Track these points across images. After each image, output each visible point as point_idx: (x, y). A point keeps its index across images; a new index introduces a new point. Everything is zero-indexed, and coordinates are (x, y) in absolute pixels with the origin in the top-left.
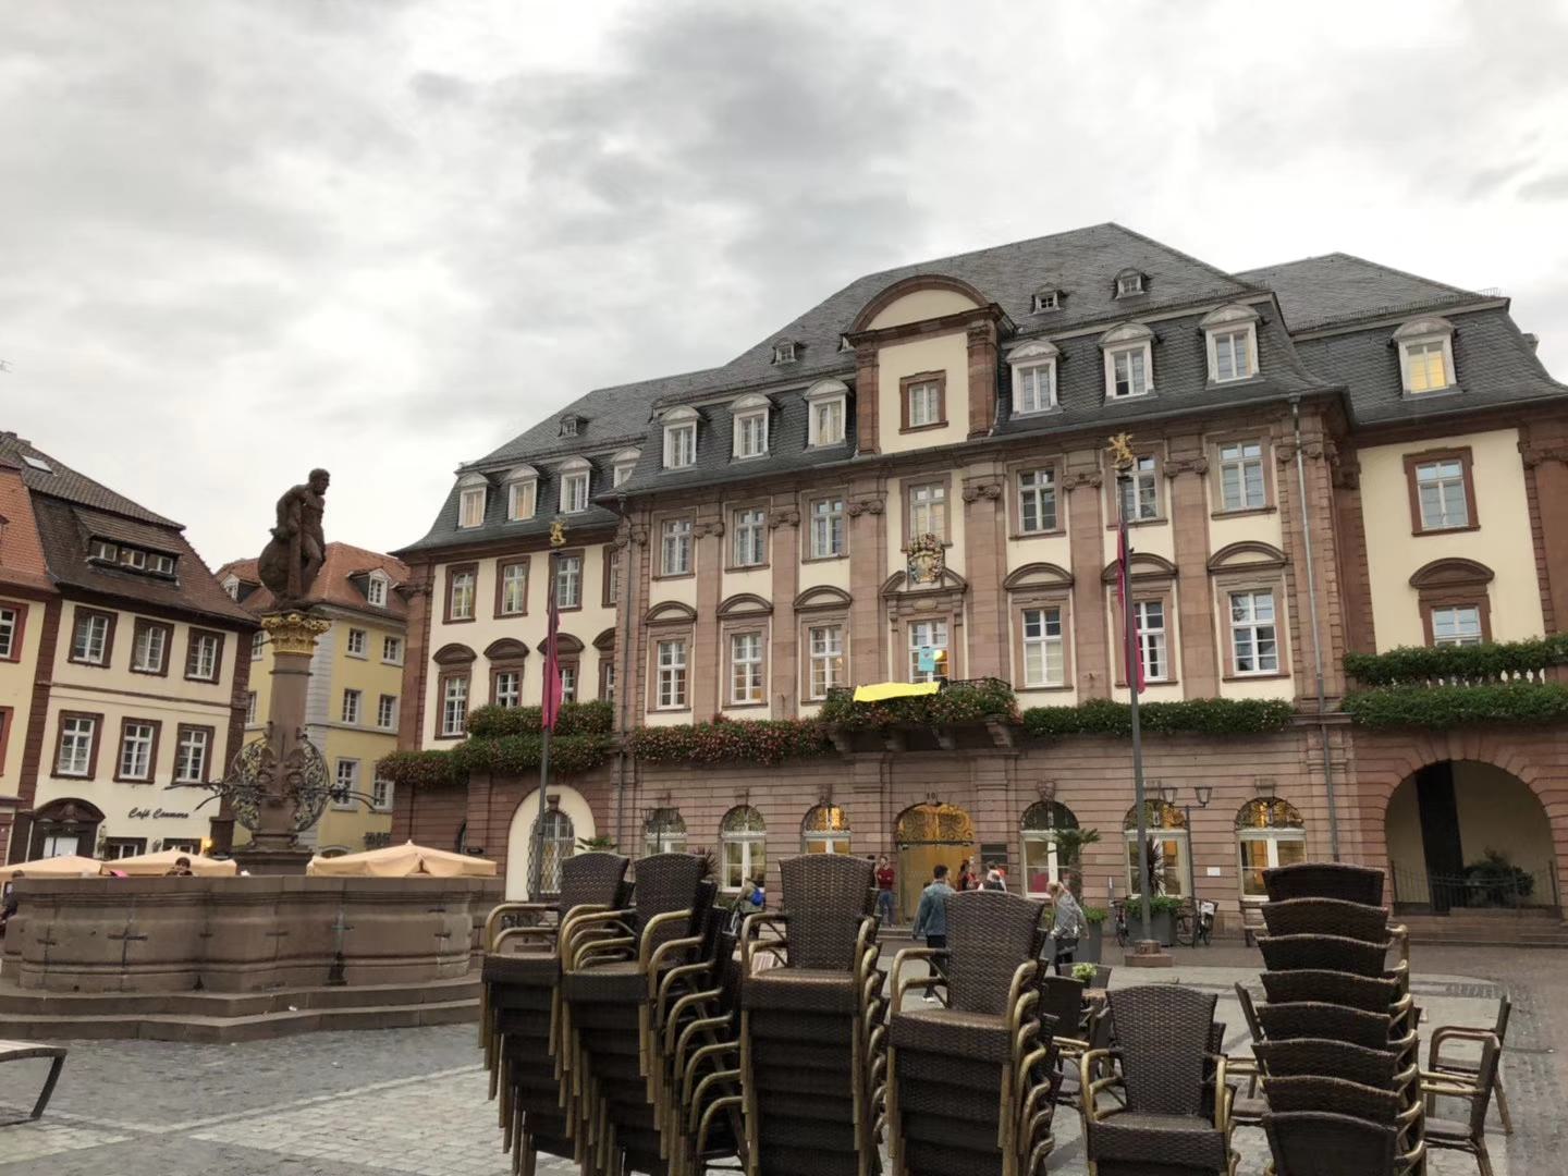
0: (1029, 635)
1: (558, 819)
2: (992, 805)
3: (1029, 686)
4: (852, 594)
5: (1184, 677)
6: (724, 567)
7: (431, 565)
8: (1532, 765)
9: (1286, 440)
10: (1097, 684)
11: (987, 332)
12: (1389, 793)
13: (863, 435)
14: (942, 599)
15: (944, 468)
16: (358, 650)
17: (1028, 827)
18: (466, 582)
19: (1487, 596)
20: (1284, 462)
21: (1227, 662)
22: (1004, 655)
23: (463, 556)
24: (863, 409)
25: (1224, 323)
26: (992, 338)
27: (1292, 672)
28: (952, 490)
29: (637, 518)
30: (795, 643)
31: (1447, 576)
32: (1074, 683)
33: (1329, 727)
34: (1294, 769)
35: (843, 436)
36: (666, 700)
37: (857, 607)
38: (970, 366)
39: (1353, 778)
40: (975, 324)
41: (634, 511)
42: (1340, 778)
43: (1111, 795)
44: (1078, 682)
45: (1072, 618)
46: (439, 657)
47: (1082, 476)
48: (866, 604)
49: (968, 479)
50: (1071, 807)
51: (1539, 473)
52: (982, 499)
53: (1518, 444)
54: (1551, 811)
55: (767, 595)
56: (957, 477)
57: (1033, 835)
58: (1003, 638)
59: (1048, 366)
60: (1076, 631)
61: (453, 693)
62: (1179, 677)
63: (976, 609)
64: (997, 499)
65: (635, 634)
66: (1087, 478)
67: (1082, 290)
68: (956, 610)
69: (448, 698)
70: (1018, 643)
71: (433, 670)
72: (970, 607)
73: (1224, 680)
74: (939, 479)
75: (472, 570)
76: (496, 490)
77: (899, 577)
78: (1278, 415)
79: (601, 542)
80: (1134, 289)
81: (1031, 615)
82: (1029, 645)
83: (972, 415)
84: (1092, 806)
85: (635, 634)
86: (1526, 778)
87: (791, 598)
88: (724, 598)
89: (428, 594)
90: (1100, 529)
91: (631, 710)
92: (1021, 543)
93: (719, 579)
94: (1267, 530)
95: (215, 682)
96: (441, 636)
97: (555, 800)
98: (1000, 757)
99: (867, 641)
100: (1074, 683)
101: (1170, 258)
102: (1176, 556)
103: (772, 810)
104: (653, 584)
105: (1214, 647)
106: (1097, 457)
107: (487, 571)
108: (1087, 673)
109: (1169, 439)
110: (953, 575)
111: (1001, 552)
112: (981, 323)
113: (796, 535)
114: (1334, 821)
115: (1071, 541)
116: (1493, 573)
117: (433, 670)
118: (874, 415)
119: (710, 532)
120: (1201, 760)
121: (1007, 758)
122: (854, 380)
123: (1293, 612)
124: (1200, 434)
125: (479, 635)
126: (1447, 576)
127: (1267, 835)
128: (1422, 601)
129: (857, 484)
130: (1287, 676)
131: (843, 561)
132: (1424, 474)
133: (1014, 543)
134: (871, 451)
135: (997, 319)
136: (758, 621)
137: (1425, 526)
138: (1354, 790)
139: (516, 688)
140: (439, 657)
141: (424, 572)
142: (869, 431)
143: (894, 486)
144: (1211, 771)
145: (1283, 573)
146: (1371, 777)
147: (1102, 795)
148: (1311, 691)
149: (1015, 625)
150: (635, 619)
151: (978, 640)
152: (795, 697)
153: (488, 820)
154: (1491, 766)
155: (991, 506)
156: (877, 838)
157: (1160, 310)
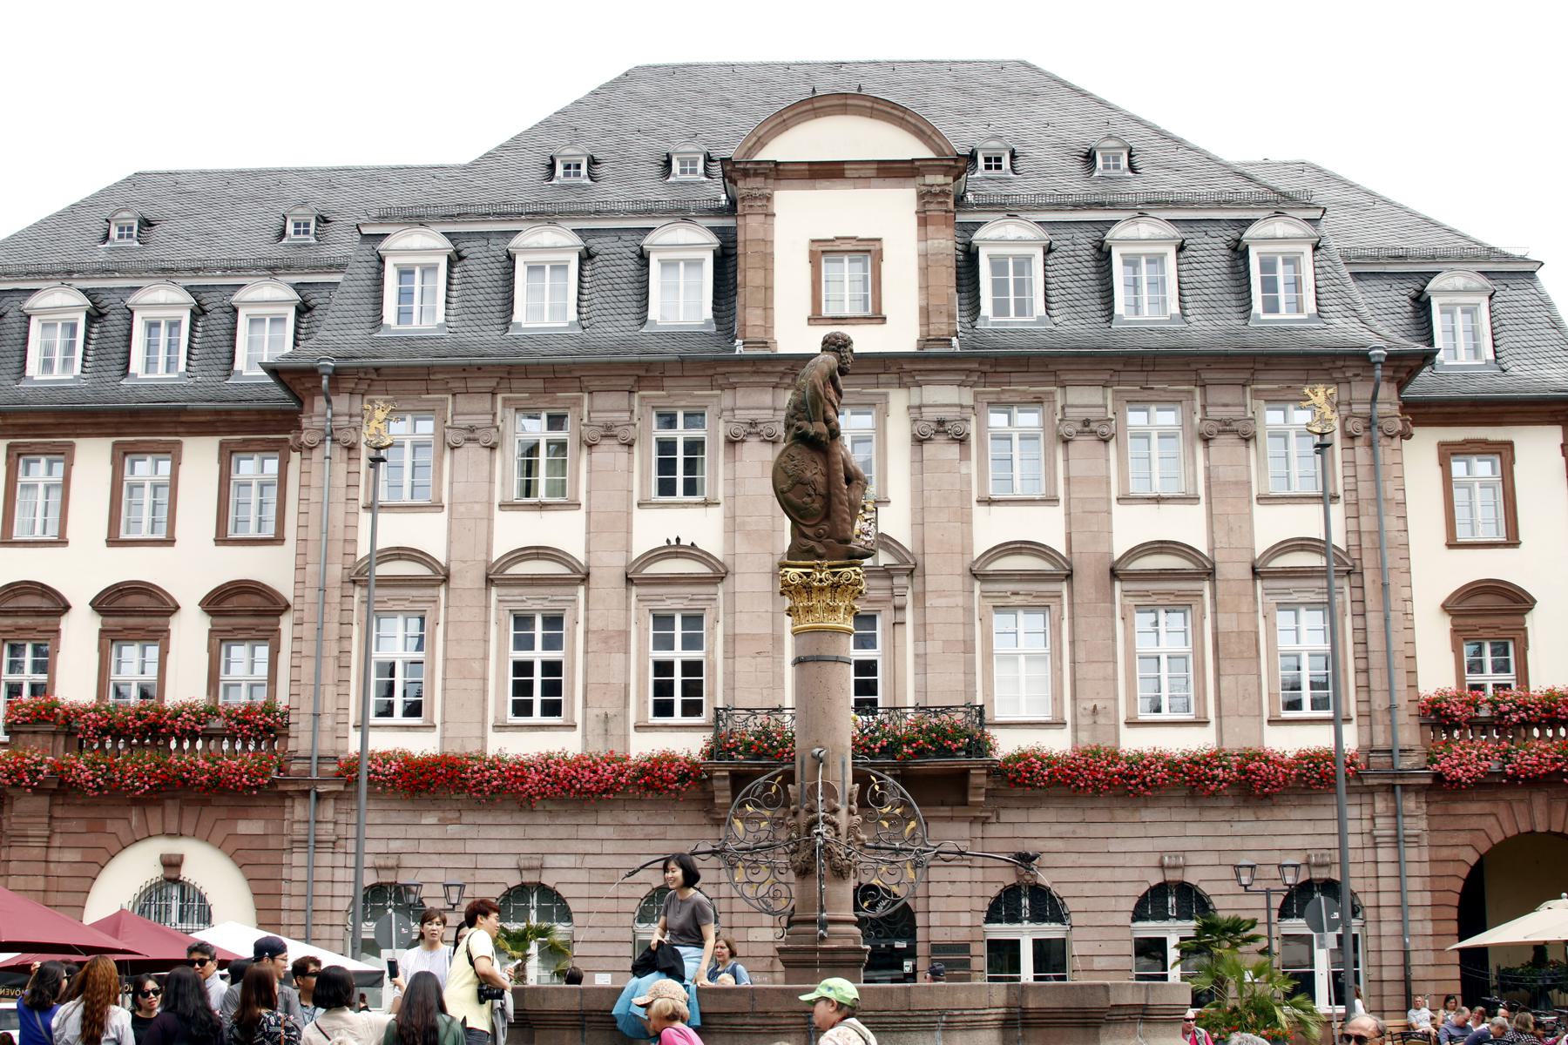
2: (949, 889)
4: (728, 562)
5: (1219, 716)
6: (497, 500)
10: (1101, 720)
12: (1464, 871)
13: (750, 317)
15: (878, 385)
17: (989, 920)
19: (1525, 630)
20: (1352, 438)
22: (969, 672)
24: (748, 275)
25: (1273, 239)
27: (1353, 714)
28: (889, 420)
29: (341, 403)
30: (626, 634)
32: (1068, 718)
33: (1405, 788)
35: (708, 313)
36: (388, 711)
38: (923, 238)
40: (930, 179)
42: (1411, 853)
43: (1118, 874)
44: (1075, 716)
47: (1086, 423)
49: (920, 407)
50: (1056, 890)
52: (941, 438)
53: (1562, 446)
55: (578, 551)
56: (898, 400)
57: (1002, 931)
59: (1029, 258)
60: (1072, 643)
62: (1211, 715)
64: (962, 440)
66: (1094, 426)
67: (1035, 153)
68: (898, 601)
72: (920, 598)
73: (1270, 722)
74: (867, 400)
78: (1349, 374)
80: (1117, 167)
83: (926, 313)
84: (1087, 889)
85: (334, 596)
88: (636, 554)
90: (1109, 500)
91: (327, 722)
92: (994, 509)
93: (490, 519)
97: (172, 864)
98: (963, 819)
100: (1068, 718)
102: (1212, 549)
103: (584, 890)
105: (1259, 676)
106: (1105, 398)
108: (1090, 706)
109: (1203, 386)
111: (966, 520)
112: (940, 179)
113: (630, 461)
114: (1402, 907)
115: (1068, 514)
116: (1534, 601)
118: (768, 288)
119: (475, 440)
120: (1239, 828)
121: (973, 820)
123: (1360, 637)
129: (740, 392)
131: (711, 510)
132: (1458, 468)
133: (986, 508)
136: (560, 592)
137: (1463, 535)
138: (1426, 869)
139: (39, 667)
142: (759, 312)
144: (1252, 843)
146: (1445, 853)
147: (1104, 874)
148: (1380, 741)
150: (336, 572)
152: (626, 717)
156: (768, 935)
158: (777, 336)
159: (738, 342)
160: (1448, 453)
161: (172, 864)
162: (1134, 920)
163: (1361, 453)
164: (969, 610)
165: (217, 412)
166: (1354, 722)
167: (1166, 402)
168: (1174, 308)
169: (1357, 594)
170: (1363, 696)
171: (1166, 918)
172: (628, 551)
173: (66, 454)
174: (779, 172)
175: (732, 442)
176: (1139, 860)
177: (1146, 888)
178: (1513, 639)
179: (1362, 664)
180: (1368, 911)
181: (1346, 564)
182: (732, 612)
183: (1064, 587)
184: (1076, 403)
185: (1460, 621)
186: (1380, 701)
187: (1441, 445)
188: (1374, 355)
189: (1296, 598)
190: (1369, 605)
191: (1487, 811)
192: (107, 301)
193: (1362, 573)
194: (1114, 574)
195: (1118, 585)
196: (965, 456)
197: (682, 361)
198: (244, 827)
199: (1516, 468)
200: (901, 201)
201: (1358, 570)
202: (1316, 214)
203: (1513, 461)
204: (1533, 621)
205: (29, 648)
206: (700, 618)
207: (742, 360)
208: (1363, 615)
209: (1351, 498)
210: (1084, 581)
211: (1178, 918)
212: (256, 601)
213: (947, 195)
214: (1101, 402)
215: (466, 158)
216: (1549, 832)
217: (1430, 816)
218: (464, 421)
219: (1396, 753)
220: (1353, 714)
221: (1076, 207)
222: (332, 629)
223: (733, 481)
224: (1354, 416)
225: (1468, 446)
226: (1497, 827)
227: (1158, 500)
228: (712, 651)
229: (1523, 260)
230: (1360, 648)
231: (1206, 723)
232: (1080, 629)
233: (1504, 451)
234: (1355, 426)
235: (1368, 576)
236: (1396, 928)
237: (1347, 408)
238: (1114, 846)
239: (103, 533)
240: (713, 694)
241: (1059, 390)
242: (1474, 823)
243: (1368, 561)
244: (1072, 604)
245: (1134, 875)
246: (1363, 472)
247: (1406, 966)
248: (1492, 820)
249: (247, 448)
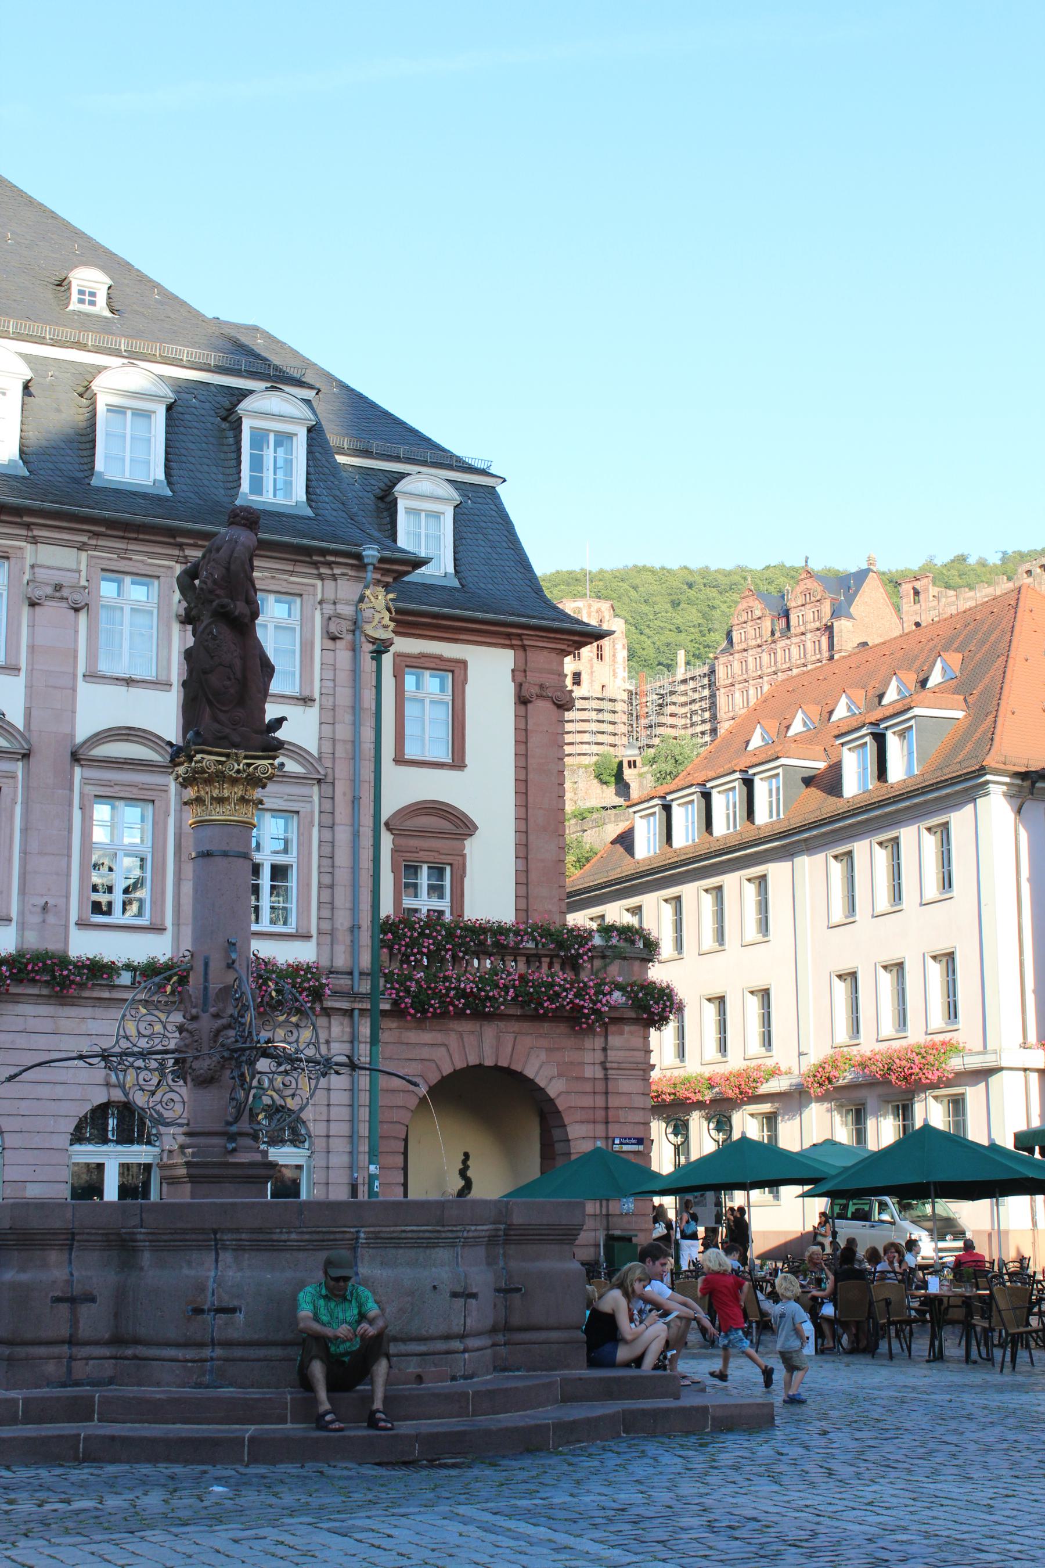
8: (560, 1075)
10: (51, 919)
19: (464, 856)
27: (314, 932)
43: (59, 1091)
44: (22, 913)
45: (18, 810)
47: (58, 587)
53: (513, 671)
60: (25, 831)
62: (169, 922)
66: (65, 593)
86: (552, 1092)
90: (75, 676)
106: (79, 563)
115: (29, 687)
116: (476, 828)
123: (327, 850)
127: (106, 1154)
130: (308, 937)
162: (71, 1145)
163: (343, 656)
166: (314, 940)
167: (142, 577)
169: (327, 805)
170: (326, 913)
171: (105, 1141)
177: (88, 1107)
178: (451, 865)
179: (327, 880)
180: (317, 1141)
181: (319, 772)
183: (19, 767)
184: (48, 563)
185: (403, 841)
186: (343, 920)
188: (368, 556)
191: (439, 1041)
193: (333, 784)
195: (77, 770)
199: (468, 688)
201: (329, 779)
203: (465, 681)
208: (332, 827)
209: (329, 702)
210: (44, 763)
211: (118, 1142)
214: (74, 567)
216: (496, 1065)
219: (356, 974)
220: (314, 932)
224: (339, 616)
225: (423, 660)
226: (448, 1059)
227: (129, 682)
230: (328, 862)
231: (161, 930)
233: (457, 670)
235: (342, 788)
237: (332, 607)
241: (29, 545)
242: (425, 1053)
243: (342, 772)
244: (27, 788)
245: (76, 1093)
246: (344, 677)
248: (443, 1051)
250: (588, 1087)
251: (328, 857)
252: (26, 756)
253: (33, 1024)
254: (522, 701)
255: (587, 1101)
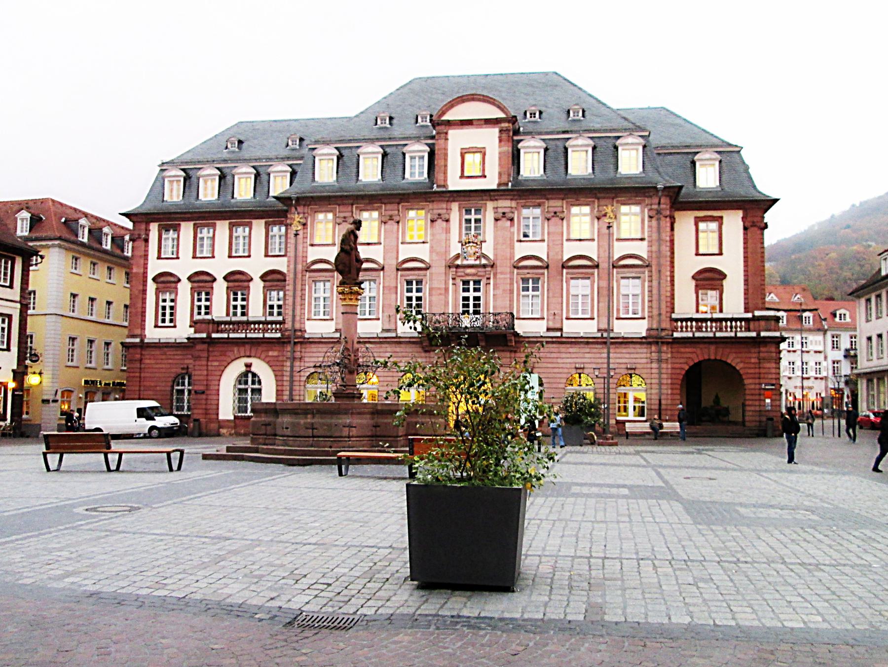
0: (523, 290)
1: (250, 375)
3: (522, 316)
5: (598, 316)
7: (148, 223)
8: (741, 362)
9: (654, 207)
10: (557, 317)
11: (509, 130)
12: (683, 372)
13: (439, 176)
14: (480, 269)
16: (76, 268)
18: (172, 234)
21: (618, 310)
22: (511, 300)
23: (169, 219)
24: (438, 162)
26: (511, 134)
30: (396, 288)
31: (707, 275)
32: (545, 317)
33: (662, 343)
34: (644, 361)
37: (433, 270)
38: (500, 147)
39: (669, 366)
41: (299, 205)
42: (664, 366)
43: (561, 370)
46: (154, 279)
48: (439, 269)
51: (749, 232)
52: (504, 219)
53: (743, 218)
54: (746, 382)
56: (490, 205)
58: (512, 292)
61: (164, 301)
62: (595, 316)
63: (499, 276)
65: (299, 276)
67: (549, 110)
69: (161, 304)
70: (518, 295)
71: (151, 287)
72: (495, 275)
75: (177, 228)
76: (189, 180)
77: (457, 257)
79: (262, 218)
81: (525, 280)
82: (523, 296)
83: (500, 174)
86: (738, 368)
87: (394, 262)
89: (146, 241)
92: (522, 244)
94: (642, 249)
95: (11, 286)
96: (155, 267)
97: (249, 366)
99: (439, 289)
101: (594, 101)
104: (310, 248)
107: (187, 229)
109: (598, 199)
110: (485, 257)
111: (512, 247)
112: (506, 125)
114: (660, 384)
117: (151, 287)
121: (511, 351)
122: (433, 144)
124: (613, 199)
125: (184, 268)
126: (707, 275)
128: (696, 286)
130: (644, 318)
132: (702, 226)
133: (519, 243)
134: (444, 186)
135: (513, 124)
137: (701, 251)
138: (669, 371)
140: (154, 279)
141: (143, 226)
142: (442, 175)
143: (455, 206)
145: (646, 270)
148: (655, 326)
149: (517, 285)
150: (300, 267)
151: (499, 292)
153: (207, 375)
154: (726, 363)
155: (509, 222)
157: (595, 131)
158: (449, 183)
159: (435, 186)
160: (698, 220)
161: (249, 366)
163: (654, 223)
164: (512, 279)
165: (263, 211)
168: (590, 170)
172: (397, 258)
173: (214, 226)
174: (449, 124)
175: (432, 221)
176: (568, 366)
182: (431, 280)
183: (546, 271)
185: (699, 282)
186: (655, 312)
187: (696, 218)
189: (628, 275)
190: (654, 278)
192: (226, 171)
194: (563, 267)
196: (512, 225)
197: (414, 193)
198: (271, 353)
200: (495, 132)
202: (646, 134)
204: (725, 282)
205: (203, 294)
206: (422, 282)
207: (435, 192)
212: (279, 277)
213: (509, 130)
215: (352, 114)
217: (672, 352)
218: (342, 215)
221: (558, 133)
222: (299, 287)
223: (433, 235)
228: (425, 294)
229: (736, 146)
231: (593, 319)
232: (551, 285)
234: (653, 213)
236: (657, 391)
238: (559, 360)
239: (227, 254)
240: (425, 308)
243: (654, 263)
246: (654, 230)
247: (660, 404)
249: (275, 224)
250: (753, 366)
251: (650, 291)
252: (547, 267)
253: (553, 350)
254: (745, 228)
255: (752, 371)
